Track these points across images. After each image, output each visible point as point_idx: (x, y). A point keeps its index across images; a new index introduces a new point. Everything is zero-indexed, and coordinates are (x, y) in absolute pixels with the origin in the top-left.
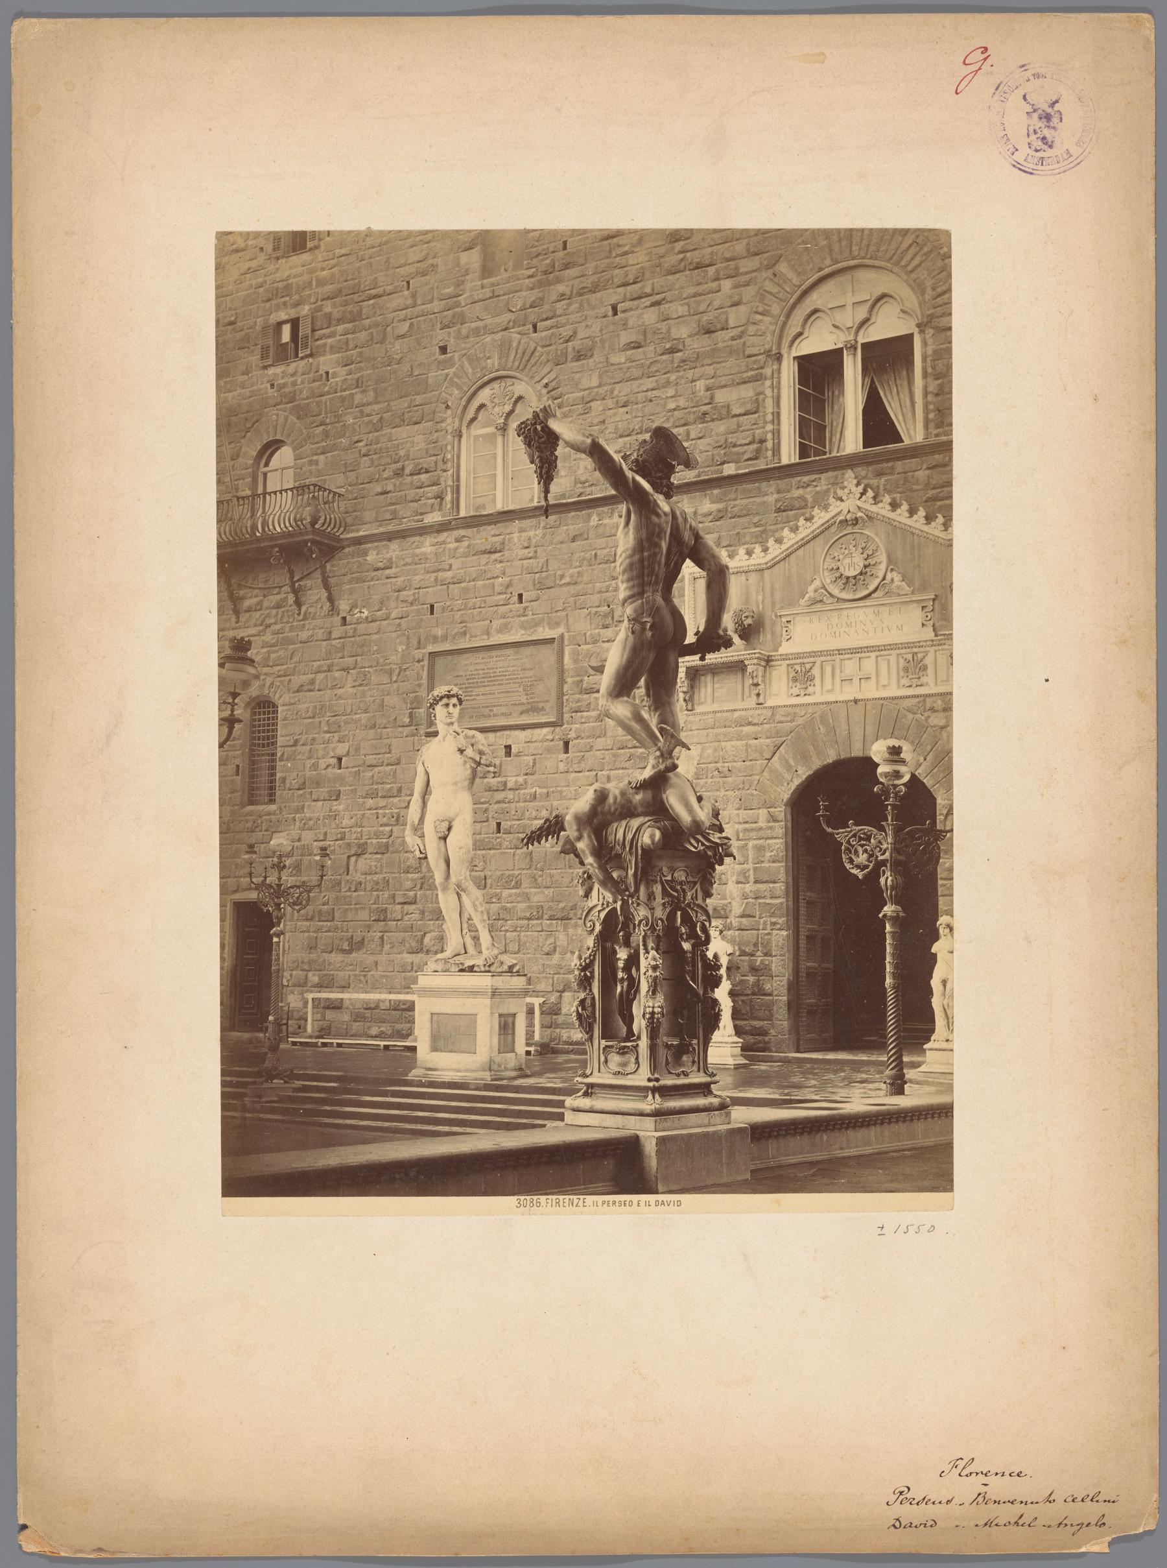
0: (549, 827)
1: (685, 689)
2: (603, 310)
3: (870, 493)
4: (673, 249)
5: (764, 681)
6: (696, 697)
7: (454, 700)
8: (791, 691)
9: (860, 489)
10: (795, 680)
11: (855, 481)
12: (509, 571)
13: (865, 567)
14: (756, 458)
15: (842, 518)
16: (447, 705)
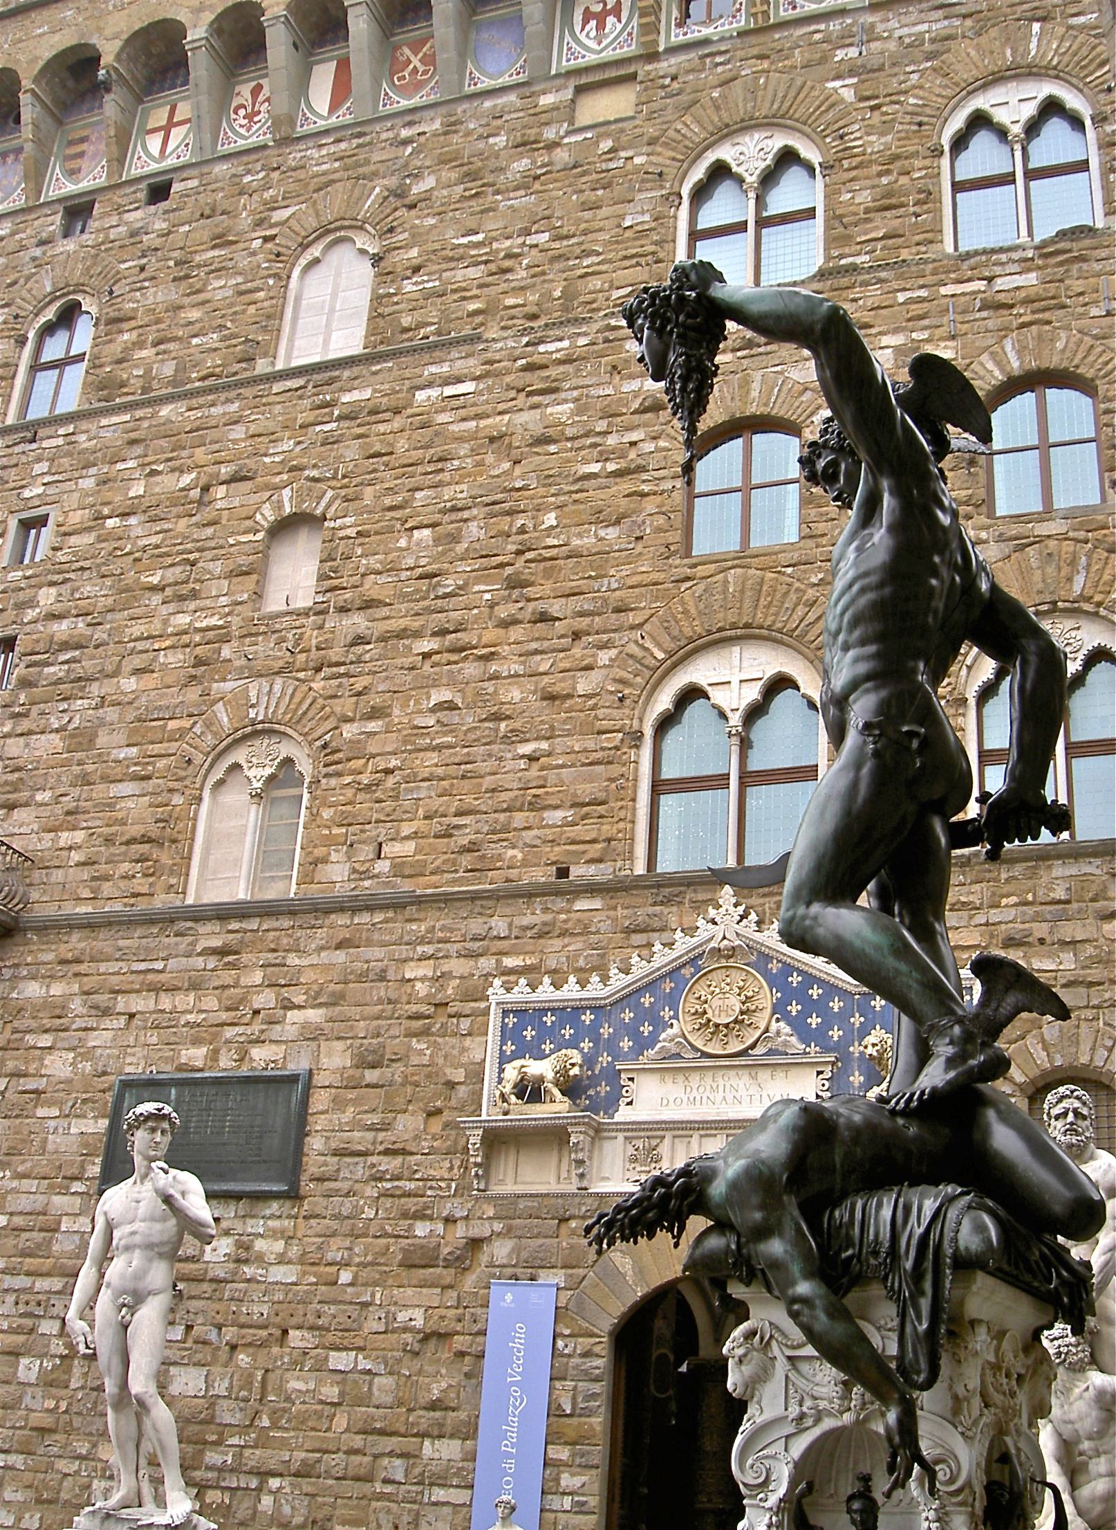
0: (666, 1198)
1: (479, 1160)
2: (410, 660)
3: (753, 917)
4: (510, 595)
5: (590, 1158)
6: (493, 1172)
7: (166, 1125)
8: (628, 1175)
9: (741, 909)
10: (634, 1160)
11: (734, 900)
12: (244, 981)
13: (742, 1013)
14: (600, 861)
15: (713, 944)
16: (153, 1130)
